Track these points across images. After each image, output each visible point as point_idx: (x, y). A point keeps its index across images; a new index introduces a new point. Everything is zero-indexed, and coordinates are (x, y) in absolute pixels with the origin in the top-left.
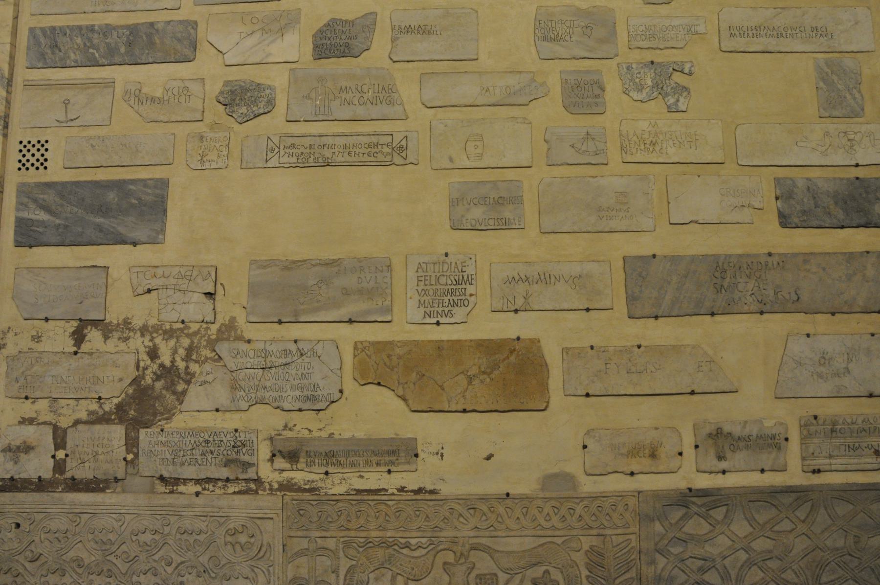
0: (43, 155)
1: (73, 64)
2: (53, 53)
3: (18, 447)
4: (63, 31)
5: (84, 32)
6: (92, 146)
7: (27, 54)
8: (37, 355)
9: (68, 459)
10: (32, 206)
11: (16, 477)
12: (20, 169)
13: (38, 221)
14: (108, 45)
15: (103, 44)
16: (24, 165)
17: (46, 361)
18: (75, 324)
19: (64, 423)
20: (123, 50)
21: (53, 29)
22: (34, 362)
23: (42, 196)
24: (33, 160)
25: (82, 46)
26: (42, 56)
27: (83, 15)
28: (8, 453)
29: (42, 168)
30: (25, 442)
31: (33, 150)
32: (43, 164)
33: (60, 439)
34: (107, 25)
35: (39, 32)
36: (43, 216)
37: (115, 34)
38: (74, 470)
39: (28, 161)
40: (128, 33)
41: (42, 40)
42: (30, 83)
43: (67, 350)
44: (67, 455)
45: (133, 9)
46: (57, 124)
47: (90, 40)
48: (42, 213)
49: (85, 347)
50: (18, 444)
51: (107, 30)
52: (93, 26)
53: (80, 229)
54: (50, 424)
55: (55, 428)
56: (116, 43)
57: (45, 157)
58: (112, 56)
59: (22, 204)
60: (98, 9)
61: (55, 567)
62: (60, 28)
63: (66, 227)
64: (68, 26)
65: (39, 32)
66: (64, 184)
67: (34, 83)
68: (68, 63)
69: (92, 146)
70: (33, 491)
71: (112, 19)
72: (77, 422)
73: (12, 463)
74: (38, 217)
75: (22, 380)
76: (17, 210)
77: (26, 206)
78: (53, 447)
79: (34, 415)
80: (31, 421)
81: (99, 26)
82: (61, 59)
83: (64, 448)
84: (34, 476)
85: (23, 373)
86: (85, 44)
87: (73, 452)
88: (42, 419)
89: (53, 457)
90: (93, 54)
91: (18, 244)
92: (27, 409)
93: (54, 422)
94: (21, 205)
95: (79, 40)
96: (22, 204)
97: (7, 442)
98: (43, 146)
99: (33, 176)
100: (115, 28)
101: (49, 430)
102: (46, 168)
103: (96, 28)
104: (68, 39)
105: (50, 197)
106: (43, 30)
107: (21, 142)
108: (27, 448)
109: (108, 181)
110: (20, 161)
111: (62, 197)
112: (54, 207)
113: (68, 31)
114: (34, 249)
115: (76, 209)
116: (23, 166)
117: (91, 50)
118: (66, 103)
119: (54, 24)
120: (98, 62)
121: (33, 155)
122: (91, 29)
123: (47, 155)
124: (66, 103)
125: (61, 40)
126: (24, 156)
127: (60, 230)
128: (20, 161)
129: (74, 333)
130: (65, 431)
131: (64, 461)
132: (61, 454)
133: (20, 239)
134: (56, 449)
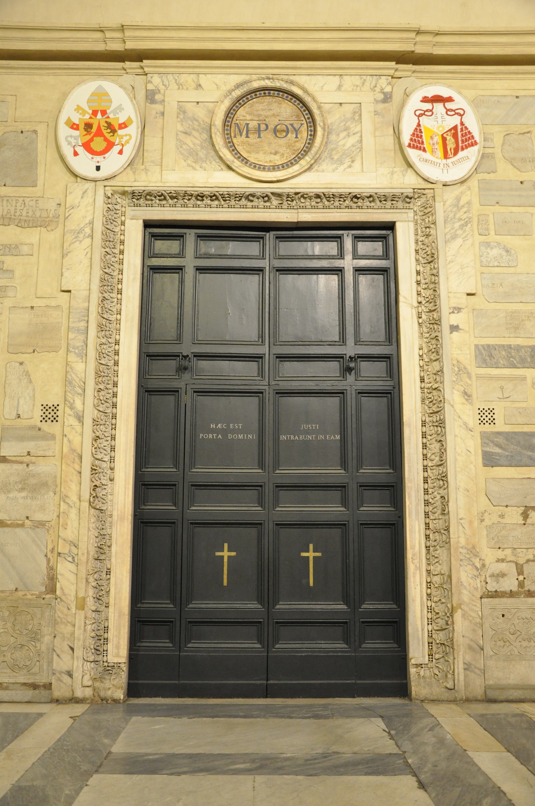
0: (492, 416)
1: (502, 366)
2: (491, 360)
3: (498, 575)
4: (494, 347)
5: (506, 348)
6: (520, 413)
7: (476, 359)
8: (503, 525)
9: (525, 580)
10: (491, 445)
11: (498, 590)
12: (480, 424)
13: (495, 453)
14: (520, 356)
15: (517, 356)
16: (482, 421)
17: (508, 528)
18: (523, 509)
19: (521, 561)
20: (529, 360)
21: (488, 346)
22: (502, 529)
23: (496, 439)
24: (487, 419)
25: (506, 356)
26: (485, 361)
27: (503, 339)
28: (493, 578)
29: (492, 423)
30: (501, 572)
31: (487, 414)
32: (493, 421)
33: (520, 571)
34: (518, 345)
35: (481, 347)
36: (497, 450)
37: (523, 350)
38: (529, 586)
39: (484, 419)
40: (530, 350)
41: (483, 352)
42: (480, 376)
43: (519, 522)
44: (525, 578)
45: (531, 336)
46: (499, 400)
47: (510, 353)
48: (497, 448)
49: (529, 521)
50: (498, 573)
51: (518, 348)
52: (510, 345)
53: (519, 458)
54: (513, 562)
55: (517, 564)
56: (525, 356)
57: (493, 417)
58: (524, 363)
59: (485, 443)
60: (512, 335)
61: (526, 637)
62: (492, 345)
63: (512, 456)
64: (496, 345)
65: (481, 347)
66: (507, 433)
67: (482, 376)
68: (500, 365)
69: (520, 413)
70: (508, 597)
71: (520, 342)
72: (528, 561)
73: (495, 583)
74: (495, 451)
75: (496, 539)
76: (482, 446)
77: (488, 444)
78: (516, 574)
79: (504, 557)
80: (503, 560)
81: (514, 345)
82: (495, 363)
83: (523, 575)
84: (508, 589)
85: (496, 535)
86: (507, 355)
87: (528, 577)
88: (508, 559)
89: (517, 579)
90: (513, 361)
91: (485, 465)
92: (500, 554)
93: (515, 561)
94: (484, 444)
95: (504, 353)
96: (485, 443)
97: (492, 571)
98: (491, 411)
99: (488, 428)
100: (523, 347)
101: (514, 565)
102: (494, 424)
103: (512, 346)
104: (498, 352)
105: (500, 440)
106: (483, 346)
107: (479, 409)
108: (503, 575)
109: (531, 432)
110: (480, 419)
111: (507, 440)
112: (503, 446)
113: (497, 347)
114: (494, 468)
115: (516, 447)
116: (482, 422)
117: (511, 359)
118: (502, 388)
119: (488, 343)
120: (516, 366)
121: (487, 416)
122: (510, 346)
123: (494, 416)
124: (502, 388)
125: (493, 352)
126: (482, 416)
127: (509, 458)
128: (480, 419)
129: (522, 514)
130: (522, 565)
131: (523, 581)
132: (521, 578)
133: (487, 463)
134: (518, 576)
